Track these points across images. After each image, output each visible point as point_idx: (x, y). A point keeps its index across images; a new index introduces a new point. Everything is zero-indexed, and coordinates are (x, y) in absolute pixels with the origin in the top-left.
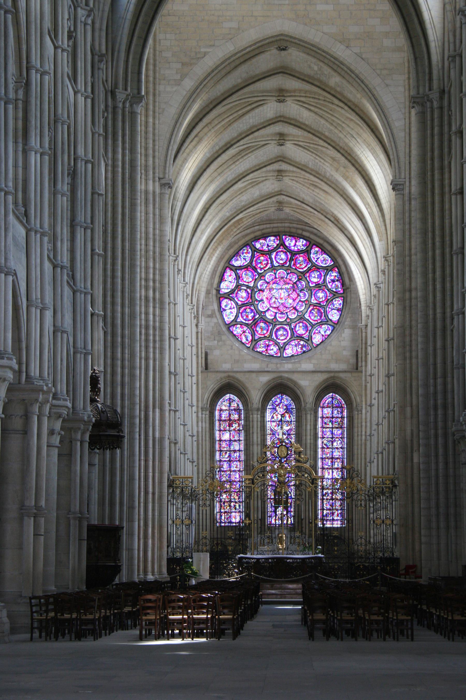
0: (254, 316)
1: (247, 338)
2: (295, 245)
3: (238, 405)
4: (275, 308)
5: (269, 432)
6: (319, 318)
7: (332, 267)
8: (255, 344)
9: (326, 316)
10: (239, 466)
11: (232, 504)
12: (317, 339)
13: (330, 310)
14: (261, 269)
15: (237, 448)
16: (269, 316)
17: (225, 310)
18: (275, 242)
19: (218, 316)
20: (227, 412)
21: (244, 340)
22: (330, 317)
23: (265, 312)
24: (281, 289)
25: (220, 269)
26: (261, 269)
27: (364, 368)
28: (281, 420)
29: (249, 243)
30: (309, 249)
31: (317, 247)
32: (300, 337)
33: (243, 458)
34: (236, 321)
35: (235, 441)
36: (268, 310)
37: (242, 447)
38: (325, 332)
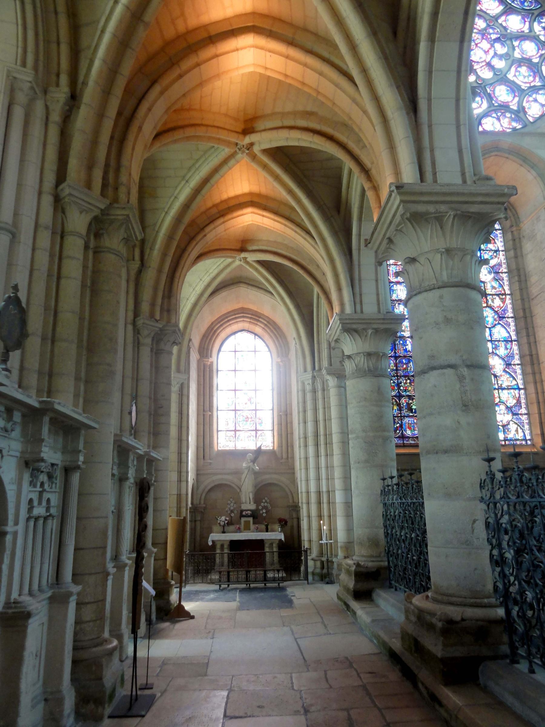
6: (531, 79)
11: (403, 400)
32: (504, 107)
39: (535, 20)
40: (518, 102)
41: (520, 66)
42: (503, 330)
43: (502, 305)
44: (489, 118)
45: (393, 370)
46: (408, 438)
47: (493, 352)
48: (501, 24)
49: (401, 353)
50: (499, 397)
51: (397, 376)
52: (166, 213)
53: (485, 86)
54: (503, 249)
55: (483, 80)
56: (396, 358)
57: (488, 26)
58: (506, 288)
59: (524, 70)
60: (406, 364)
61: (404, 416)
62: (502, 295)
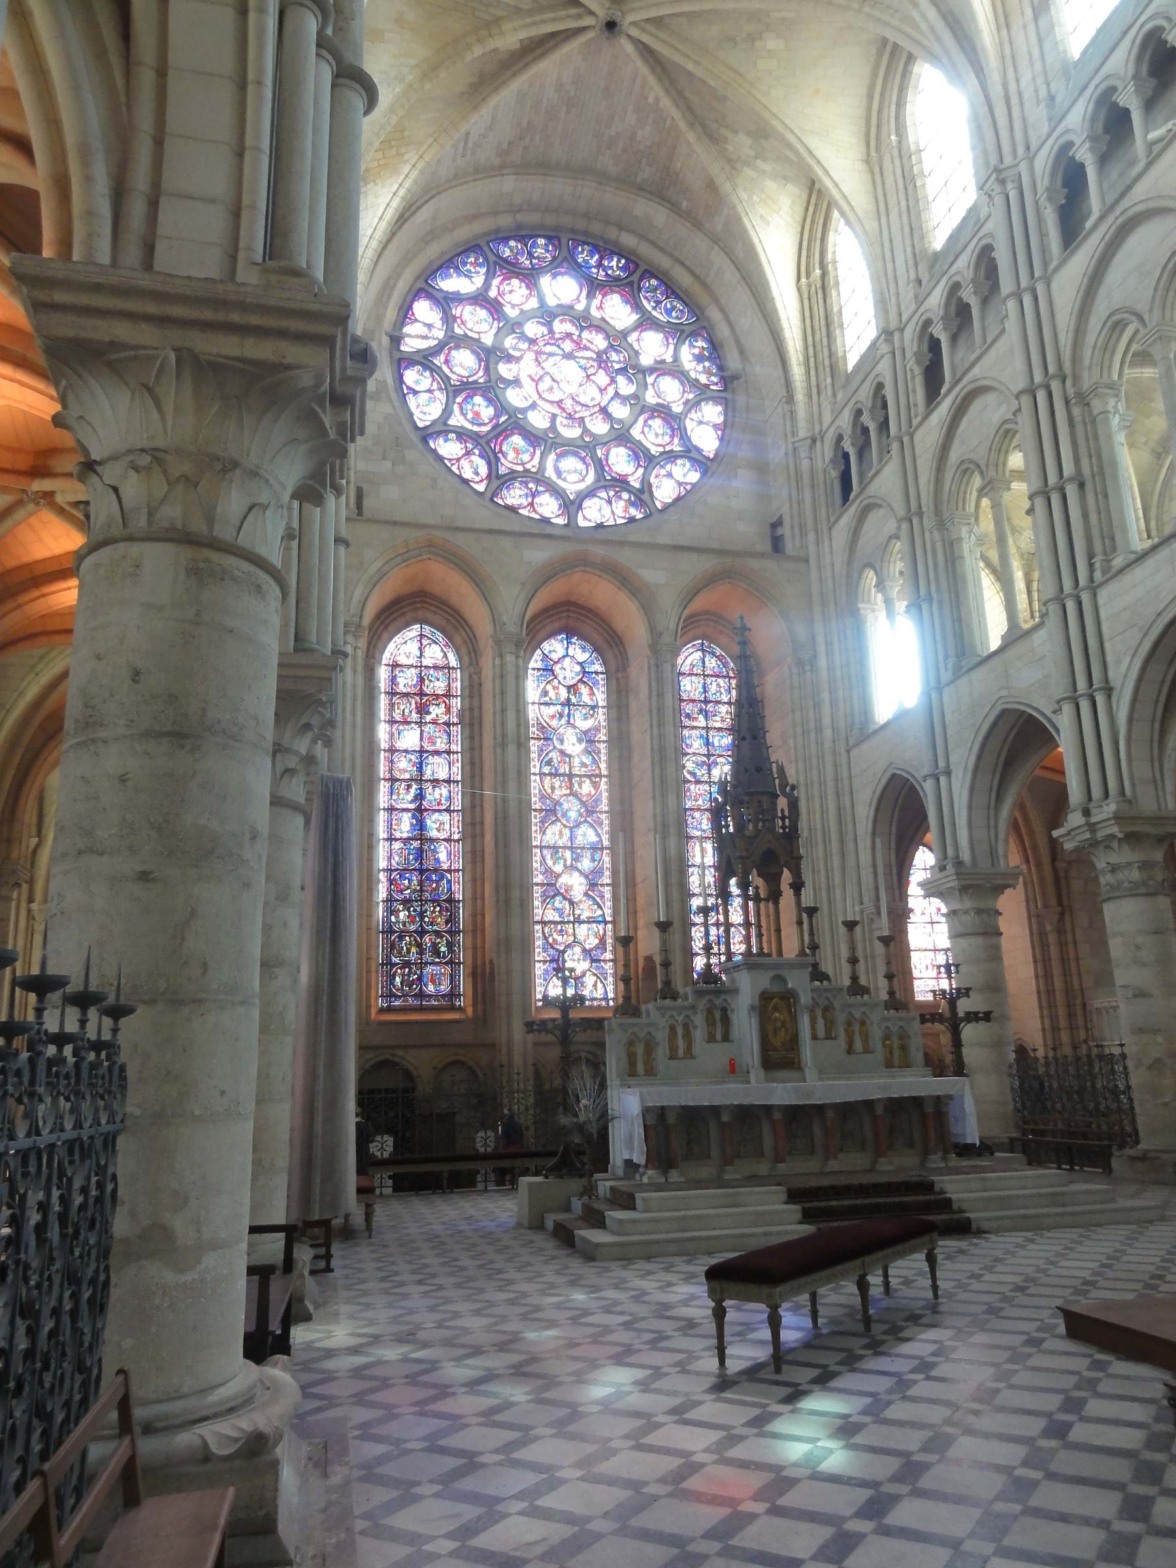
0: (497, 416)
1: (474, 469)
2: (599, 265)
3: (445, 656)
4: (552, 402)
5: (533, 731)
6: (667, 439)
7: (693, 327)
8: (499, 488)
9: (685, 437)
10: (447, 827)
11: (427, 938)
12: (665, 492)
13: (695, 423)
14: (513, 306)
15: (442, 774)
16: (538, 420)
17: (415, 393)
18: (547, 251)
19: (397, 404)
20: (413, 670)
21: (468, 474)
22: (696, 441)
23: (524, 411)
24: (569, 356)
25: (402, 285)
26: (513, 306)
27: (812, 548)
28: (568, 703)
29: (482, 243)
30: (635, 278)
31: (657, 278)
32: (621, 483)
33: (457, 805)
34: (445, 424)
35: (437, 753)
36: (533, 406)
37: (457, 772)
38: (685, 475)
39: (684, 343)
40: (644, 474)
41: (652, 417)
42: (591, 832)
43: (593, 792)
44: (596, 500)
45: (415, 891)
46: (431, 996)
47: (572, 865)
48: (631, 346)
49: (430, 864)
50: (574, 935)
51: (421, 900)
52: (8, 711)
53: (594, 447)
54: (605, 704)
55: (592, 435)
56: (422, 871)
57: (611, 346)
58: (603, 766)
59: (657, 423)
60: (437, 882)
61: (426, 963)
62: (596, 776)
